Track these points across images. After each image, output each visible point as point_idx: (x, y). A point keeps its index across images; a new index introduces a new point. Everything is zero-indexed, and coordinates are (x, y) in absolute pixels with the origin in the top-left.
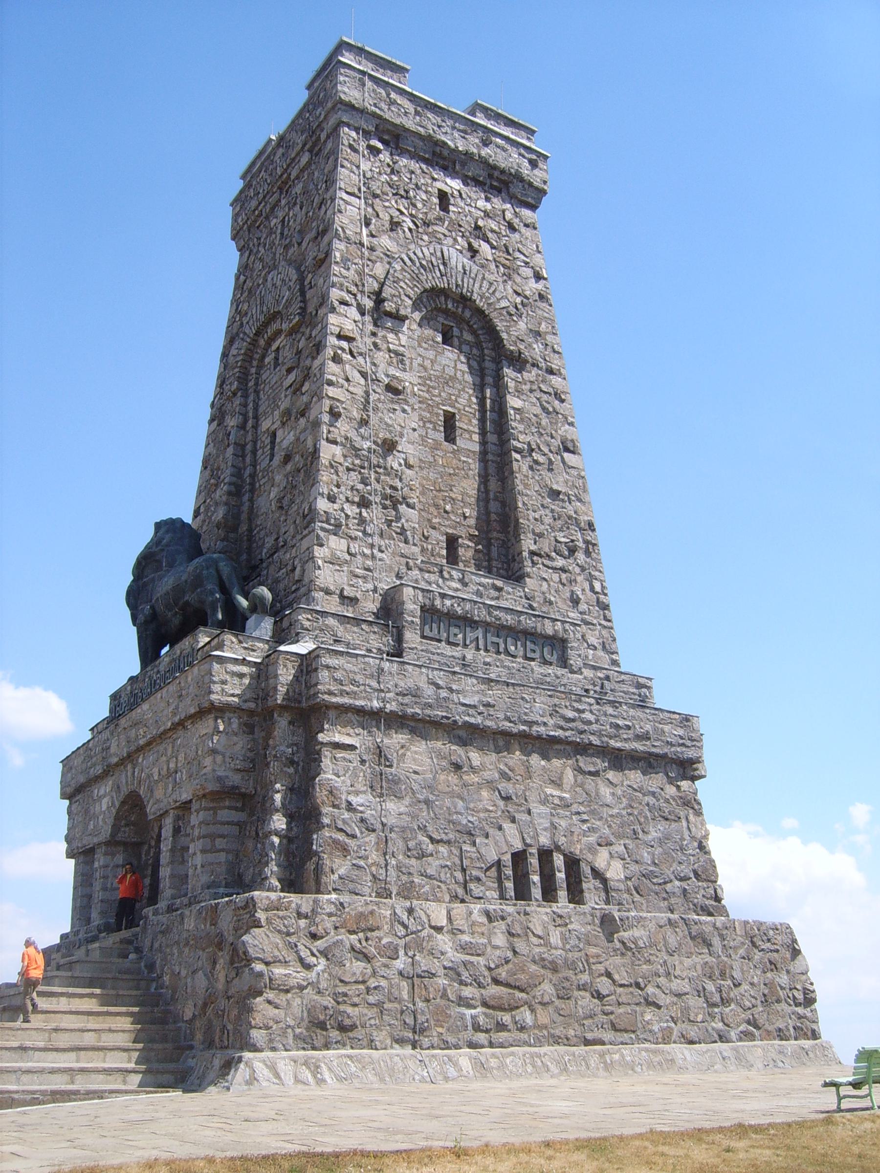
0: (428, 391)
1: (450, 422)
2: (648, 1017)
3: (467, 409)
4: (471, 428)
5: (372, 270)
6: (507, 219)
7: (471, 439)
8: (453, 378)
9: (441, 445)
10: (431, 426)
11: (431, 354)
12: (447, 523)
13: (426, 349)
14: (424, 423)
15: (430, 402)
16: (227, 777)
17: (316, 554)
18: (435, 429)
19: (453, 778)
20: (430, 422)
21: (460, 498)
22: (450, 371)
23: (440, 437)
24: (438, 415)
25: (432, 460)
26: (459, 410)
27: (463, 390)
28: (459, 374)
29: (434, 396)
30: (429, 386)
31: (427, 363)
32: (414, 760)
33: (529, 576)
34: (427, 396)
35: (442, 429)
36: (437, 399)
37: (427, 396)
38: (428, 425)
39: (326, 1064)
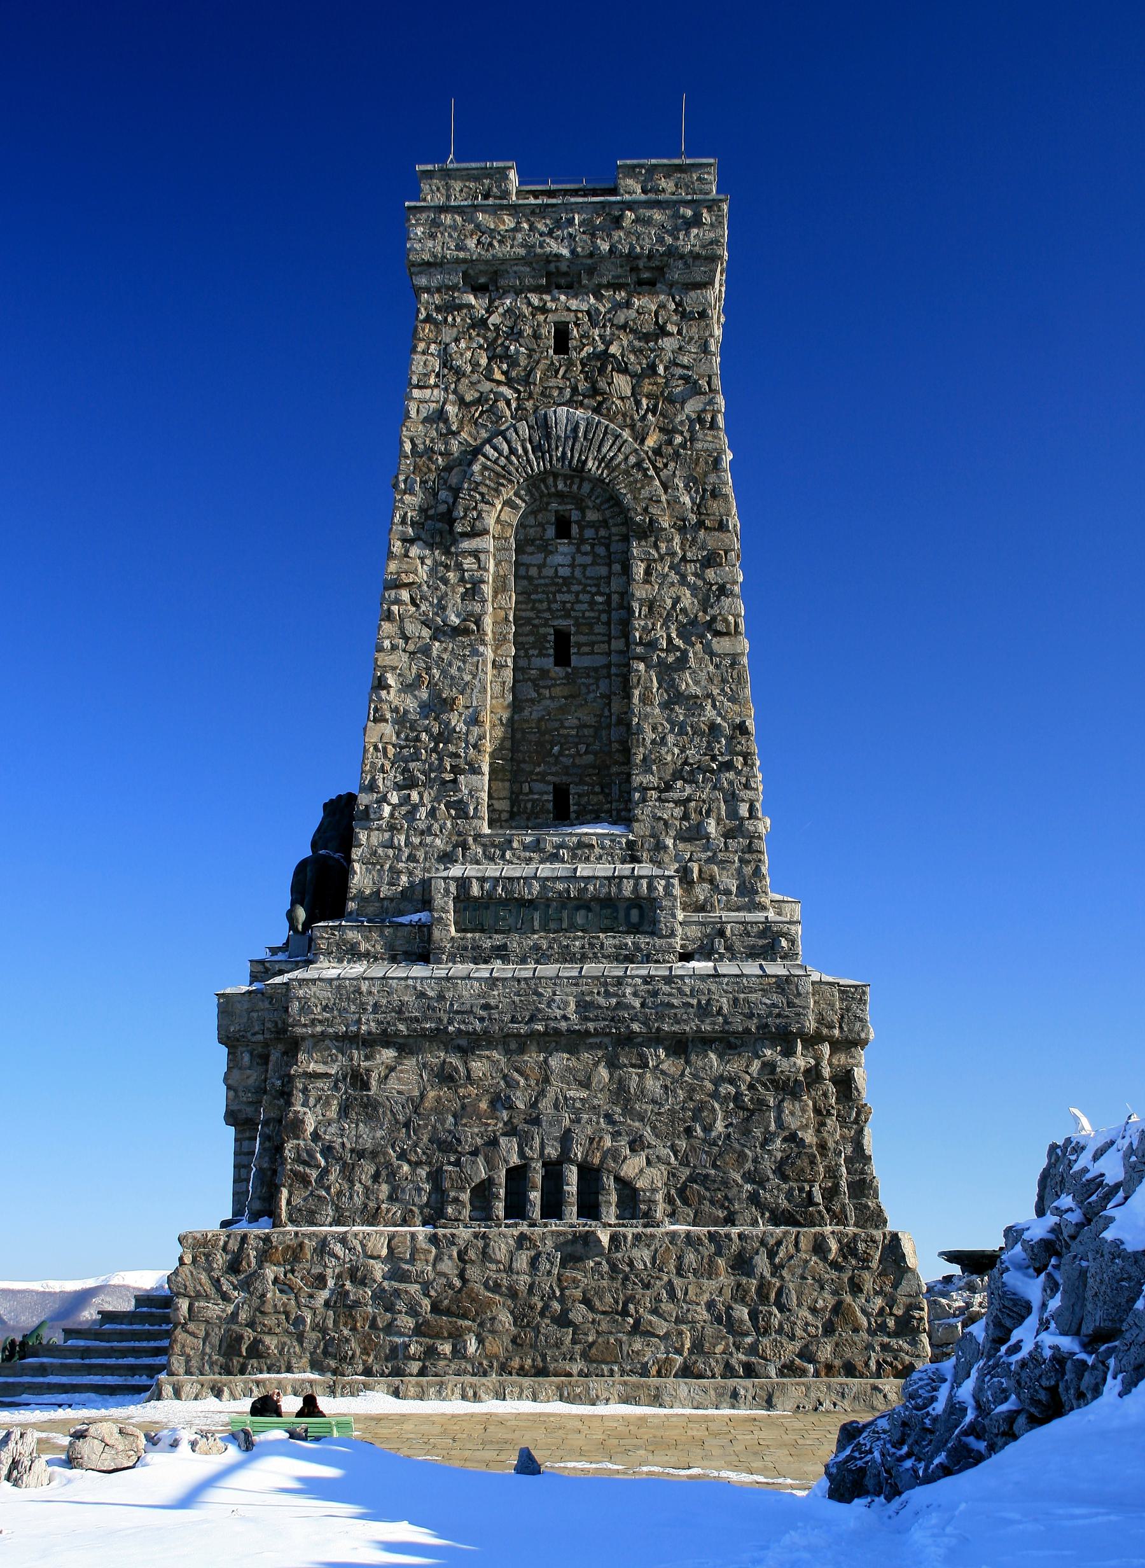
0: (533, 609)
1: (562, 641)
2: (637, 1346)
3: (587, 614)
4: (594, 638)
5: (445, 482)
6: (660, 321)
7: (592, 653)
8: (567, 581)
9: (548, 671)
10: (536, 652)
11: (538, 558)
12: (554, 769)
13: (532, 554)
14: (526, 651)
15: (536, 622)
16: (240, 1111)
17: (354, 857)
18: (541, 655)
19: (445, 1092)
20: (533, 648)
21: (574, 732)
22: (564, 572)
23: (548, 663)
24: (545, 636)
25: (534, 695)
26: (576, 618)
27: (584, 591)
28: (578, 573)
29: (539, 611)
30: (535, 601)
31: (533, 572)
32: (399, 1079)
33: (638, 820)
34: (531, 614)
35: (551, 651)
36: (547, 615)
37: (531, 614)
38: (531, 652)
39: (229, 1388)
